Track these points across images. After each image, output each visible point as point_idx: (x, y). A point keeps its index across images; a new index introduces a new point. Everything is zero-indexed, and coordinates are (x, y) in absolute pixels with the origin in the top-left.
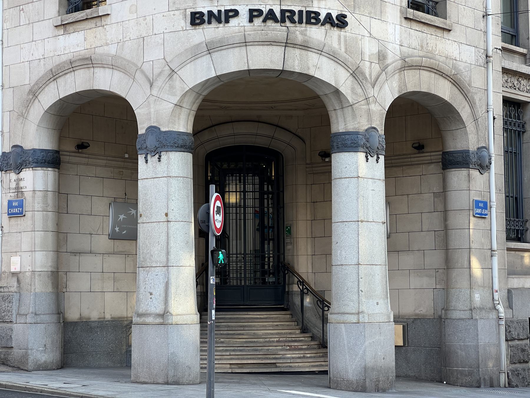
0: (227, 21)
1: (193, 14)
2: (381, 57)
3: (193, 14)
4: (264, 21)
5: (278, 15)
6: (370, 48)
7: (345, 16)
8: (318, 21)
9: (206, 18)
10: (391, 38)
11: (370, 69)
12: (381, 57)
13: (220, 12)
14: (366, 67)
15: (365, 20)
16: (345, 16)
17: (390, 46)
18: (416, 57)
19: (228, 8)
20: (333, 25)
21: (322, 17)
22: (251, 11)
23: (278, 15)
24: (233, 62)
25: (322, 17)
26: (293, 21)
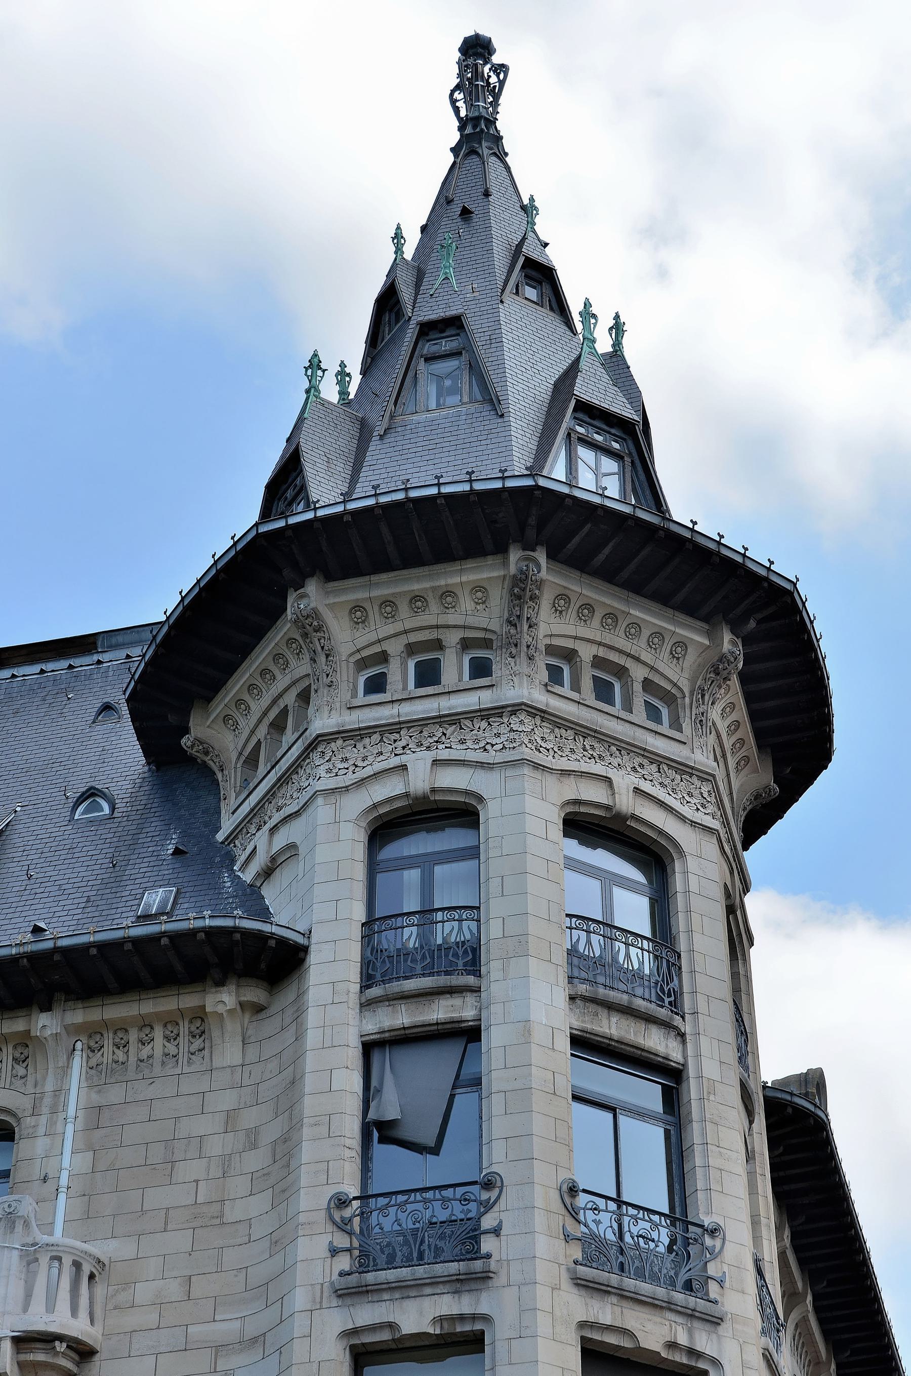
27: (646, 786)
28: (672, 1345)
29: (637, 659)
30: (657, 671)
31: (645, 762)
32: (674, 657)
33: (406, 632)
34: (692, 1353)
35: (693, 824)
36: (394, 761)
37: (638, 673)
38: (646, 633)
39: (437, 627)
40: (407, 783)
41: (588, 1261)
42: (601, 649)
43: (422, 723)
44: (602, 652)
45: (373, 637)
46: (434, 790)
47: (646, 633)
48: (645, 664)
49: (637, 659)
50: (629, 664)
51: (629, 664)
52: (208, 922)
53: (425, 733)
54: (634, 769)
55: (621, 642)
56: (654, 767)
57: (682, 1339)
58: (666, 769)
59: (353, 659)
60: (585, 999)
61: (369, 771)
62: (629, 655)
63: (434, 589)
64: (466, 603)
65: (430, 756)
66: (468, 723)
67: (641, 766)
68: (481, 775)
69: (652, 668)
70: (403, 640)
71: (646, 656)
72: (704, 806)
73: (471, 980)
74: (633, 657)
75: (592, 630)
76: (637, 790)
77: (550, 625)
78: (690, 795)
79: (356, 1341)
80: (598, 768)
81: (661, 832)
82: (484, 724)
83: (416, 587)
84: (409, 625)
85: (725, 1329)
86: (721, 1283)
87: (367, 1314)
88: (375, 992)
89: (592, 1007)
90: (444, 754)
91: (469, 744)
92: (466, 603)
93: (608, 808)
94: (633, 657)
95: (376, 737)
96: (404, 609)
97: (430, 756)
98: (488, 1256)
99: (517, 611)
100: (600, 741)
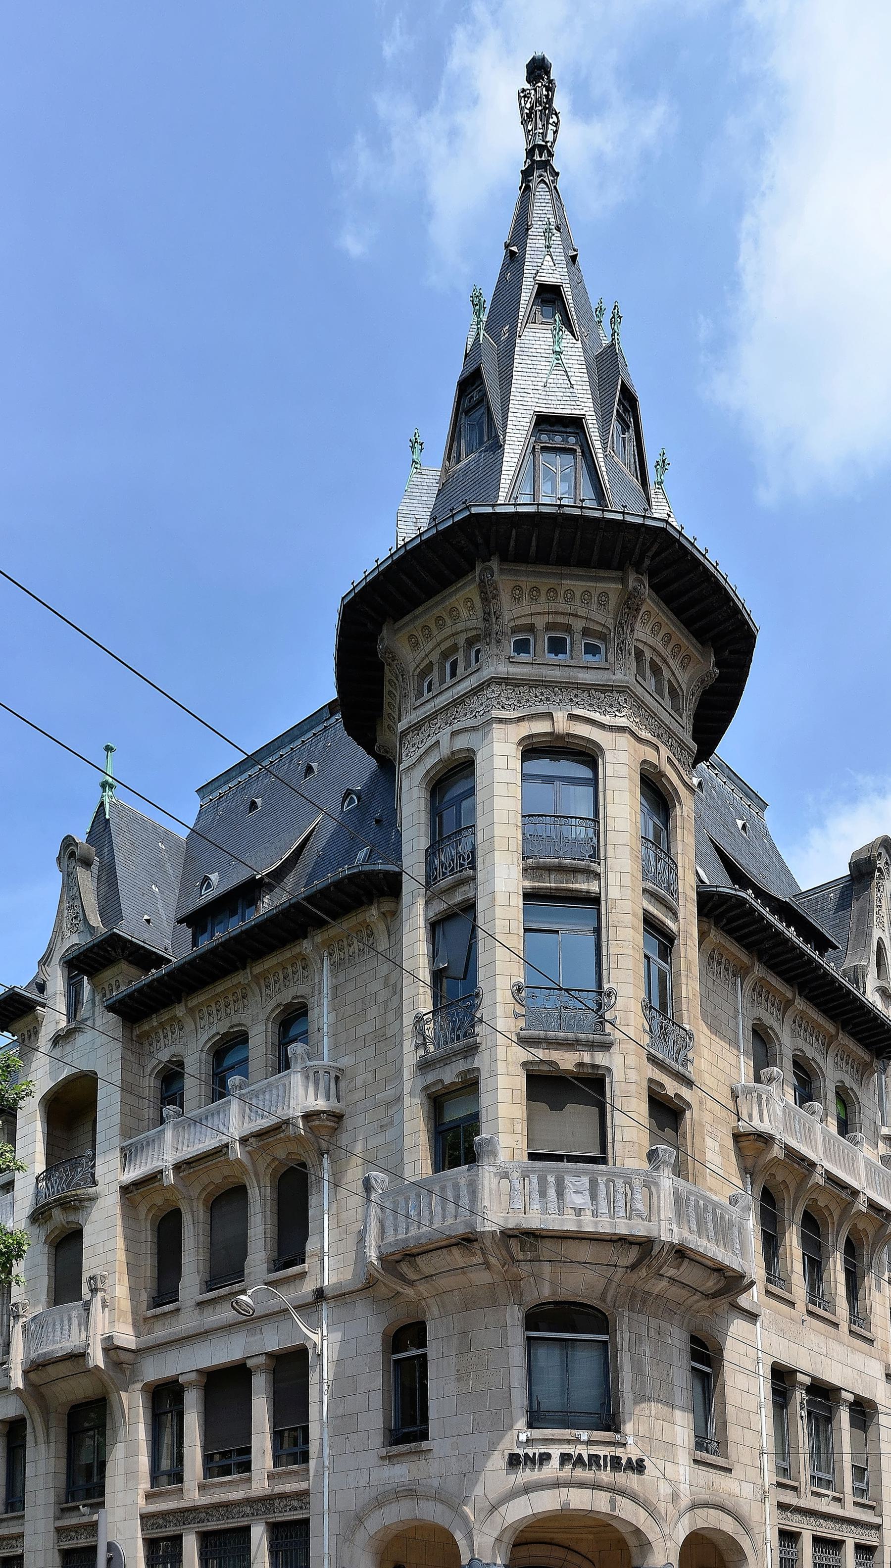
0: (541, 1464)
1: (511, 1456)
2: (675, 1496)
3: (511, 1456)
4: (574, 1465)
5: (586, 1459)
6: (665, 1489)
7: (642, 1460)
8: (620, 1464)
9: (522, 1459)
10: (682, 1479)
11: (665, 1508)
12: (675, 1496)
13: (534, 1454)
14: (661, 1506)
15: (659, 1463)
16: (642, 1460)
17: (682, 1487)
18: (703, 1496)
19: (542, 1451)
20: (633, 1469)
21: (624, 1462)
22: (563, 1456)
23: (586, 1459)
24: (547, 1502)
25: (624, 1462)
26: (599, 1466)
27: (577, 711)
29: (576, 616)
30: (590, 619)
31: (579, 692)
32: (601, 605)
36: (433, 740)
37: (578, 625)
39: (453, 635)
42: (551, 616)
43: (445, 709)
44: (551, 619)
46: (453, 753)
48: (581, 617)
49: (576, 616)
50: (571, 621)
51: (571, 621)
55: (563, 607)
56: (585, 694)
58: (594, 692)
60: (532, 868)
62: (570, 614)
65: (448, 730)
71: (581, 612)
74: (573, 615)
80: (542, 708)
85: (615, 1049)
87: (431, 1078)
89: (538, 872)
90: (456, 727)
93: (551, 734)
94: (573, 615)
97: (448, 730)
100: (547, 687)
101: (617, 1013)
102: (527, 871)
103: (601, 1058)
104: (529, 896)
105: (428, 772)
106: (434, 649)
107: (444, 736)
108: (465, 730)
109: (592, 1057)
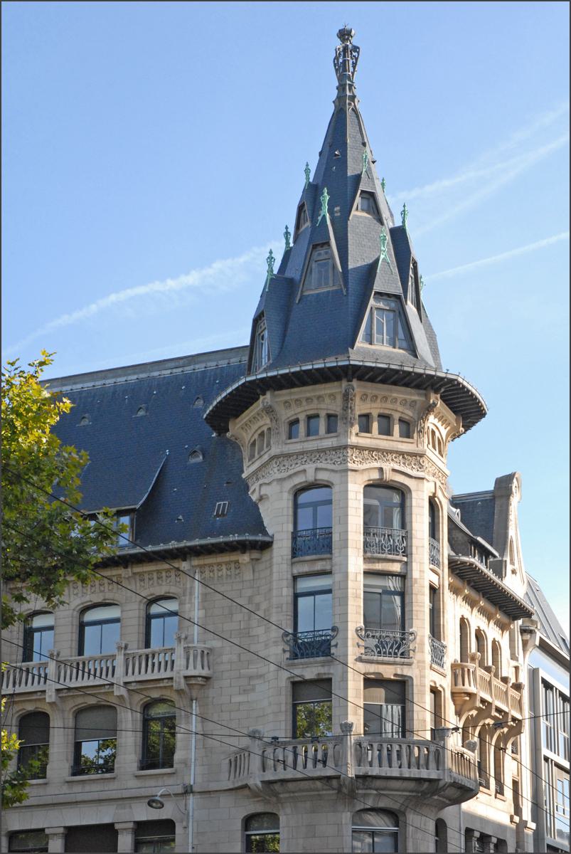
28: (395, 675)
29: (396, 411)
33: (306, 411)
34: (402, 676)
35: (416, 478)
36: (302, 468)
37: (396, 416)
38: (399, 401)
40: (306, 477)
41: (366, 654)
44: (382, 411)
45: (293, 413)
47: (399, 401)
49: (396, 411)
50: (393, 413)
51: (393, 413)
52: (237, 538)
53: (313, 456)
54: (393, 460)
55: (391, 406)
57: (399, 672)
59: (286, 421)
60: (368, 558)
61: (291, 472)
63: (315, 396)
64: (327, 400)
65: (314, 466)
66: (328, 452)
67: (396, 458)
68: (333, 474)
69: (402, 413)
70: (305, 414)
71: (400, 409)
72: (420, 468)
73: (328, 556)
75: (378, 404)
76: (394, 470)
77: (360, 408)
78: (415, 464)
79: (292, 680)
81: (402, 484)
82: (334, 453)
83: (308, 395)
84: (306, 408)
86: (414, 651)
88: (295, 559)
91: (329, 461)
92: (327, 400)
95: (295, 457)
96: (304, 403)
98: (333, 654)
99: (346, 405)
101: (417, 645)
102: (366, 560)
103: (406, 671)
104: (367, 573)
105: (295, 485)
106: (302, 412)
107: (310, 468)
108: (326, 470)
109: (402, 669)
